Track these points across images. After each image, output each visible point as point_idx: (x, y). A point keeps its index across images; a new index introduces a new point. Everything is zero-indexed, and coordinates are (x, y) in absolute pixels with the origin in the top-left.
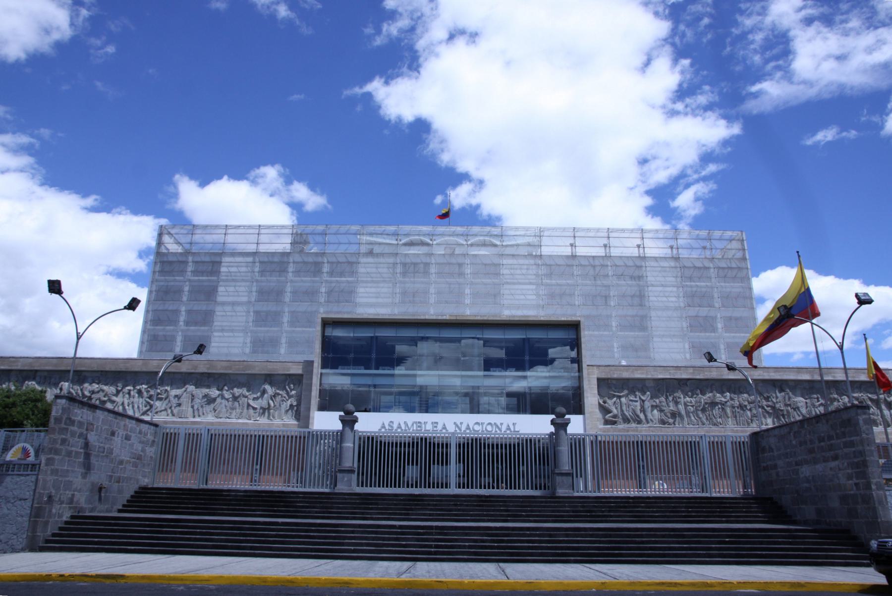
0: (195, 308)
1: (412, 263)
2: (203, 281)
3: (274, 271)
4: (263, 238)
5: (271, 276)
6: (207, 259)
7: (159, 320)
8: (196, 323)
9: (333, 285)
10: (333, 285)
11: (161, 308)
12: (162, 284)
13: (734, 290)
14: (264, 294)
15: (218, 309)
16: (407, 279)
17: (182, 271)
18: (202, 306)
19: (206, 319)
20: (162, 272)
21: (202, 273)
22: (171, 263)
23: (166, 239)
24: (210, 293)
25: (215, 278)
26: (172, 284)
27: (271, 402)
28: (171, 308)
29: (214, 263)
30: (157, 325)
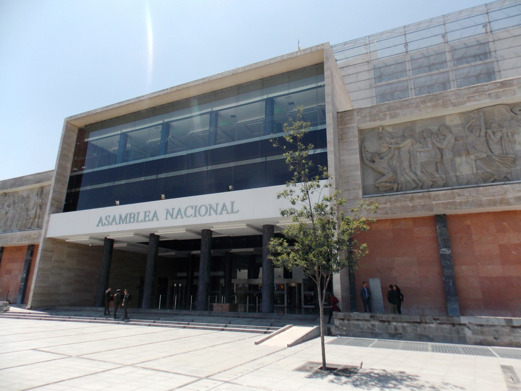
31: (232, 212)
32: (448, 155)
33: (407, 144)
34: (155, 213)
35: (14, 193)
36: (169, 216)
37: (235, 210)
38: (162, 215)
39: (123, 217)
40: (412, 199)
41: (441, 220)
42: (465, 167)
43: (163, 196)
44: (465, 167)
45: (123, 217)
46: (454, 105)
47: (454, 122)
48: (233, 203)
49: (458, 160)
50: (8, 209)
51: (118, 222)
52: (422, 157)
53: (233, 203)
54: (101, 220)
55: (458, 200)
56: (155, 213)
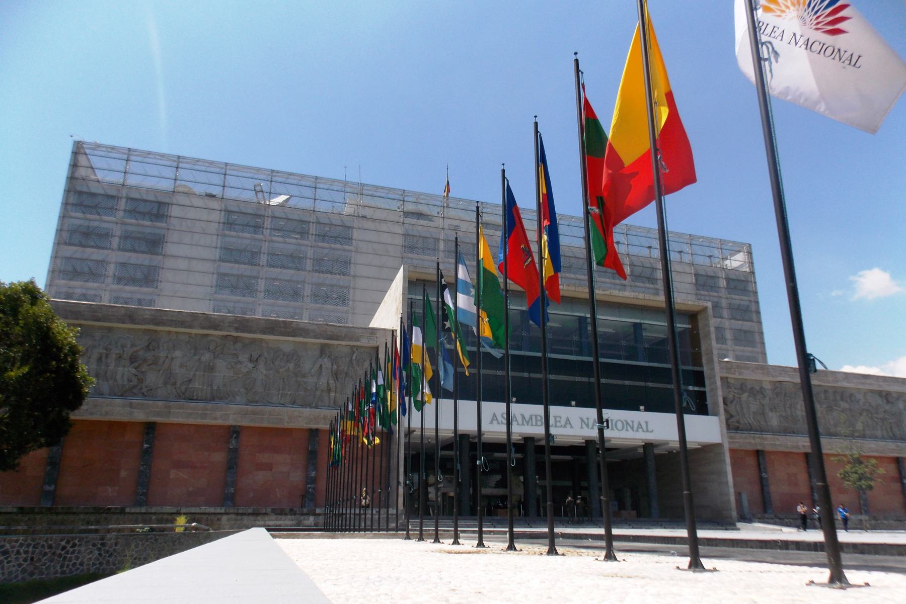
0: (133, 261)
1: (420, 237)
2: (143, 226)
3: (247, 225)
4: (230, 181)
5: (243, 231)
6: (151, 197)
7: (75, 270)
8: (133, 281)
9: (326, 251)
10: (326, 251)
11: (78, 255)
12: (78, 222)
13: (742, 303)
14: (230, 254)
15: (169, 263)
16: (415, 256)
17: (112, 208)
18: (144, 259)
19: (149, 278)
20: (79, 205)
21: (143, 215)
22: (93, 195)
23: (82, 160)
24: (155, 244)
25: (164, 225)
26: (96, 224)
27: (331, 381)
28: (94, 257)
29: (160, 204)
30: (71, 279)
31: (647, 431)
32: (767, 410)
33: (746, 395)
34: (568, 419)
35: (254, 341)
36: (584, 425)
37: (650, 429)
38: (576, 423)
39: (527, 418)
40: (754, 438)
41: (758, 453)
42: (774, 420)
43: (573, 403)
44: (774, 420)
45: (527, 418)
46: (773, 377)
47: (767, 386)
48: (646, 423)
49: (770, 414)
50: (251, 365)
51: (520, 422)
52: (754, 407)
53: (646, 423)
54: (494, 415)
55: (777, 443)
56: (568, 419)
